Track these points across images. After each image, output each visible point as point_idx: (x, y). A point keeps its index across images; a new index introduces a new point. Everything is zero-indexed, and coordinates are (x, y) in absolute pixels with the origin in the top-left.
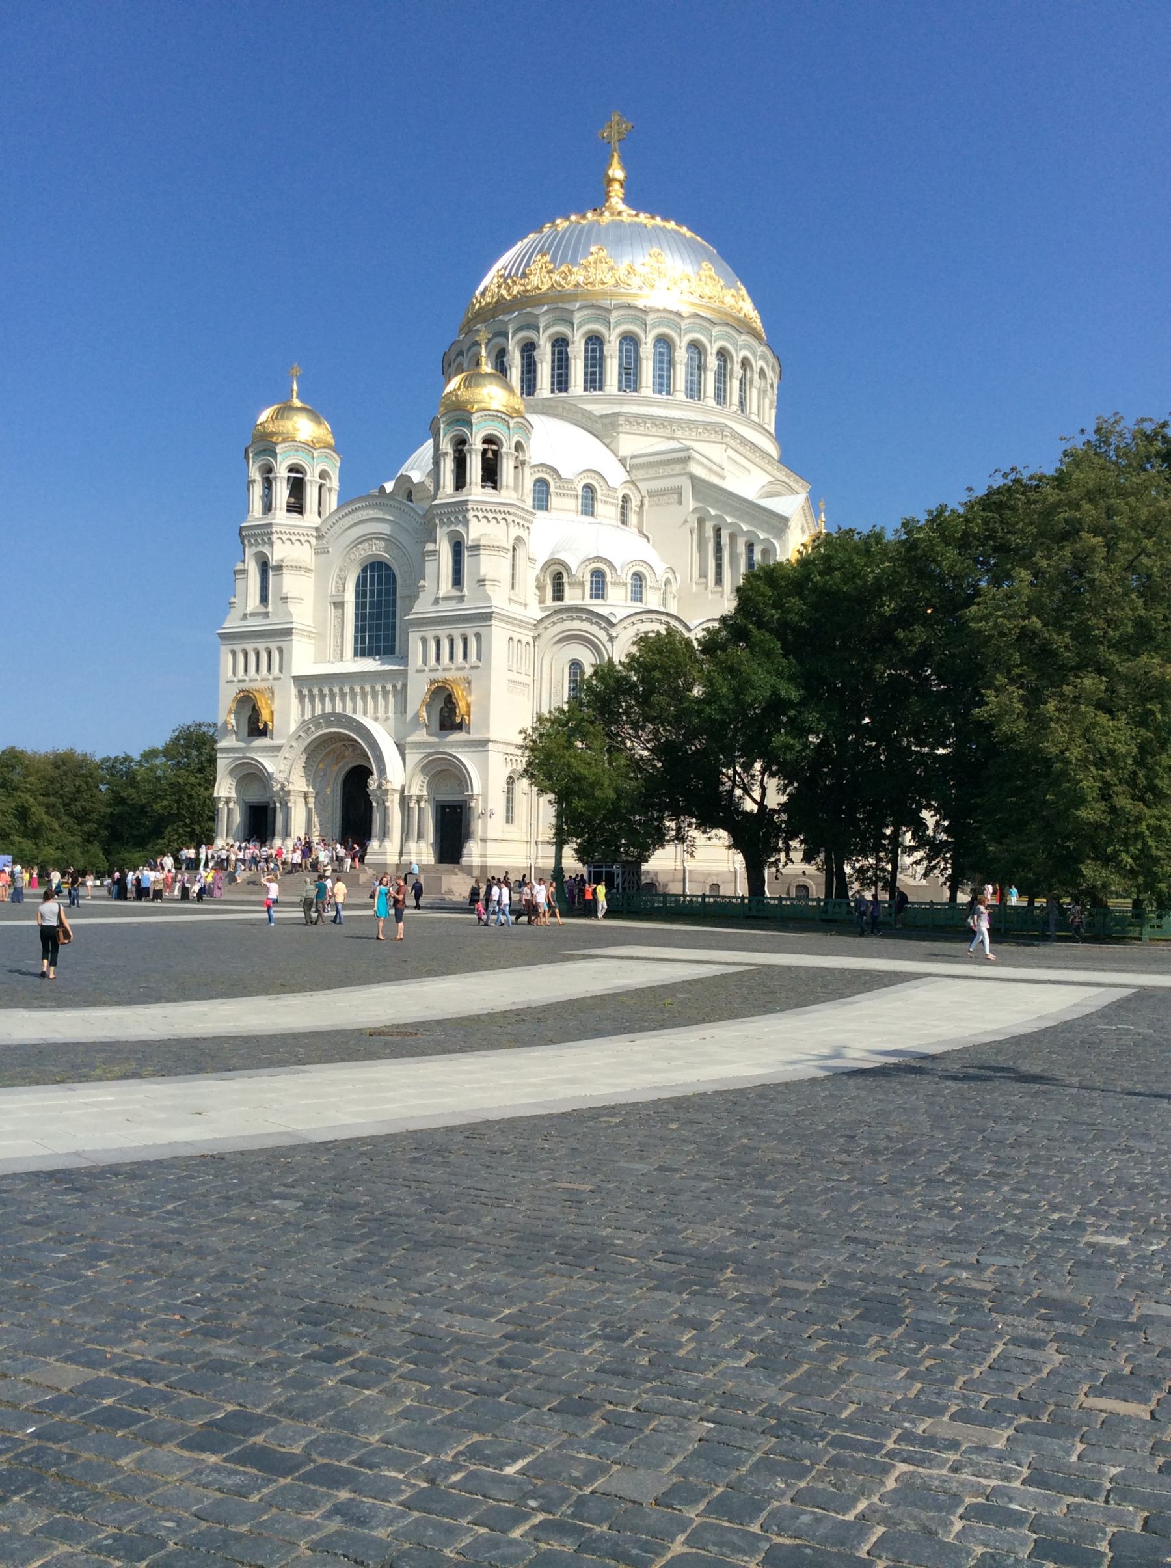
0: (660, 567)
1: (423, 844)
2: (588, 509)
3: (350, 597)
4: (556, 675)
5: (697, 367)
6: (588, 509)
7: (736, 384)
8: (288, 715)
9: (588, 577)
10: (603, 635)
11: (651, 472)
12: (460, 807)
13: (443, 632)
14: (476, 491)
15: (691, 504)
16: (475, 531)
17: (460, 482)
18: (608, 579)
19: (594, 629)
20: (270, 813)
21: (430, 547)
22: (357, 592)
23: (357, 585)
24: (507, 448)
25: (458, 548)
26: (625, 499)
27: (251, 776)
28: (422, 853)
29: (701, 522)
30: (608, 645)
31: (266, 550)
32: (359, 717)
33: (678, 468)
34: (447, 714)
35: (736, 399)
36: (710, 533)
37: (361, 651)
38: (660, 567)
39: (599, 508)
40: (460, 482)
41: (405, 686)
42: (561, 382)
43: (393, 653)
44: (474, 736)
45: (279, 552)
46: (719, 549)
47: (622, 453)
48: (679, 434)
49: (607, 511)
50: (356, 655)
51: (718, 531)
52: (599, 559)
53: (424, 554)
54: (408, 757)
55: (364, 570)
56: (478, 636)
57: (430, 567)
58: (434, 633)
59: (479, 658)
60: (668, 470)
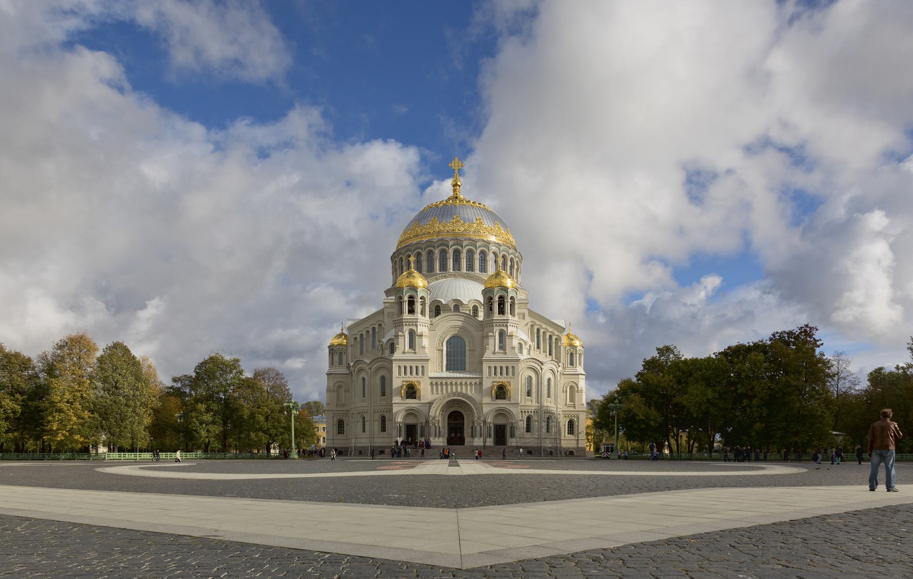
4: (523, 381)
5: (512, 267)
8: (426, 393)
13: (498, 365)
15: (528, 319)
16: (510, 330)
19: (536, 365)
21: (491, 334)
25: (502, 334)
28: (490, 442)
31: (414, 328)
32: (469, 393)
34: (501, 392)
36: (535, 331)
41: (481, 383)
42: (470, 267)
44: (512, 401)
45: (421, 329)
46: (538, 337)
50: (447, 369)
51: (538, 330)
53: (487, 337)
56: (513, 367)
57: (491, 341)
59: (513, 374)
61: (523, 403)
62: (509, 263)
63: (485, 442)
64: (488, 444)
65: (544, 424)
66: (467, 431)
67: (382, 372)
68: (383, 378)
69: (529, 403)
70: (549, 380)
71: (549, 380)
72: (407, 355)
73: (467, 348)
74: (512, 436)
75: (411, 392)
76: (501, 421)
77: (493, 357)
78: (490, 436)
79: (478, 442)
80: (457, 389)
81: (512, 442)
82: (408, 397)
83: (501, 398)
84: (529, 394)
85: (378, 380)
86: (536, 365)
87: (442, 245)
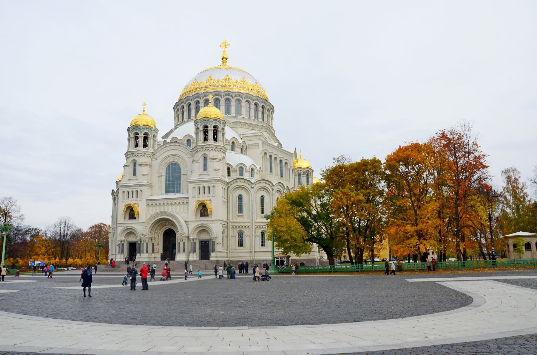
0: (258, 167)
1: (195, 254)
2: (233, 149)
3: (164, 174)
5: (256, 110)
6: (233, 149)
7: (266, 115)
9: (238, 170)
10: (249, 187)
11: (249, 139)
12: (208, 241)
14: (211, 141)
16: (211, 154)
17: (206, 139)
18: (244, 170)
19: (246, 185)
20: (137, 246)
22: (166, 173)
23: (166, 170)
24: (220, 129)
26: (242, 146)
27: (130, 232)
28: (194, 257)
29: (265, 153)
30: (251, 189)
33: (258, 138)
34: (203, 210)
35: (266, 120)
37: (167, 192)
38: (258, 167)
39: (236, 149)
40: (206, 139)
41: (187, 202)
43: (180, 192)
45: (140, 160)
47: (239, 133)
48: (255, 128)
49: (237, 150)
50: (166, 192)
52: (239, 164)
54: (189, 226)
55: (169, 166)
58: (198, 186)
60: (254, 138)
61: (235, 220)
62: (261, 109)
64: (191, 259)
69: (240, 220)
70: (262, 198)
71: (262, 198)
72: (131, 182)
73: (182, 173)
74: (213, 251)
75: (131, 213)
76: (204, 237)
77: (197, 178)
80: (168, 209)
81: (213, 257)
82: (130, 218)
83: (205, 216)
84: (240, 211)
86: (246, 185)
87: (196, 97)
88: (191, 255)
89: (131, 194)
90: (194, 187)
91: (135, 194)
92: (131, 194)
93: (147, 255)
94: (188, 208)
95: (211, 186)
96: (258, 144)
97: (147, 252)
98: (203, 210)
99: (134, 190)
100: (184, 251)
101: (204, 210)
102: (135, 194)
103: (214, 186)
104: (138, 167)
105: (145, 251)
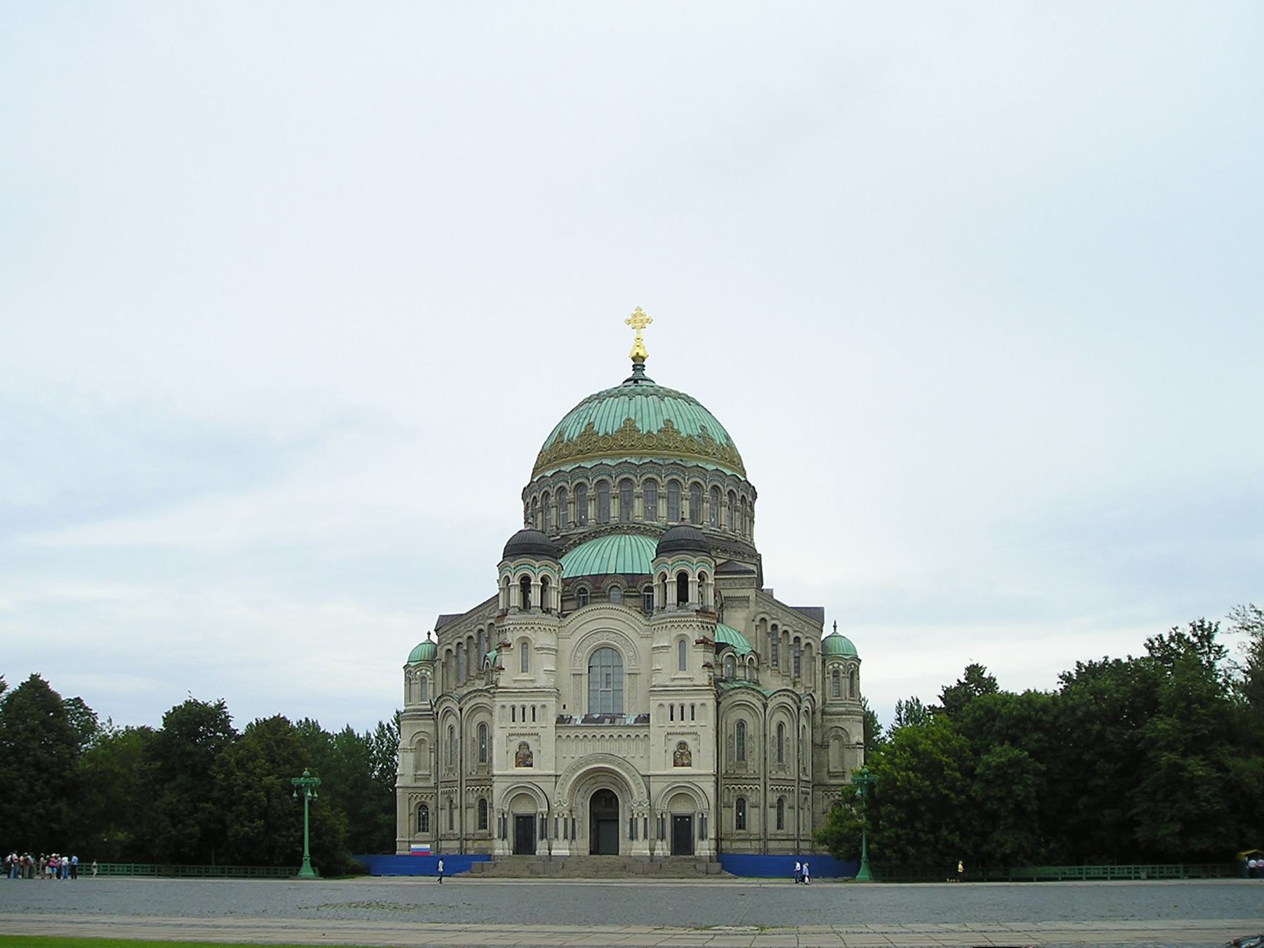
10: (759, 704)
12: (689, 817)
19: (754, 701)
28: (663, 848)
63: (652, 849)
65: (772, 814)
66: (624, 828)
67: (481, 717)
68: (482, 727)
71: (780, 727)
78: (663, 838)
79: (640, 848)
83: (683, 765)
85: (474, 732)
86: (754, 701)
88: (659, 842)
89: (519, 712)
90: (661, 705)
91: (529, 712)
92: (519, 712)
93: (566, 843)
94: (647, 750)
95: (698, 703)
96: (747, 599)
97: (566, 837)
98: (682, 756)
99: (528, 705)
100: (645, 836)
101: (682, 754)
102: (529, 712)
103: (703, 704)
104: (532, 652)
105: (561, 835)
